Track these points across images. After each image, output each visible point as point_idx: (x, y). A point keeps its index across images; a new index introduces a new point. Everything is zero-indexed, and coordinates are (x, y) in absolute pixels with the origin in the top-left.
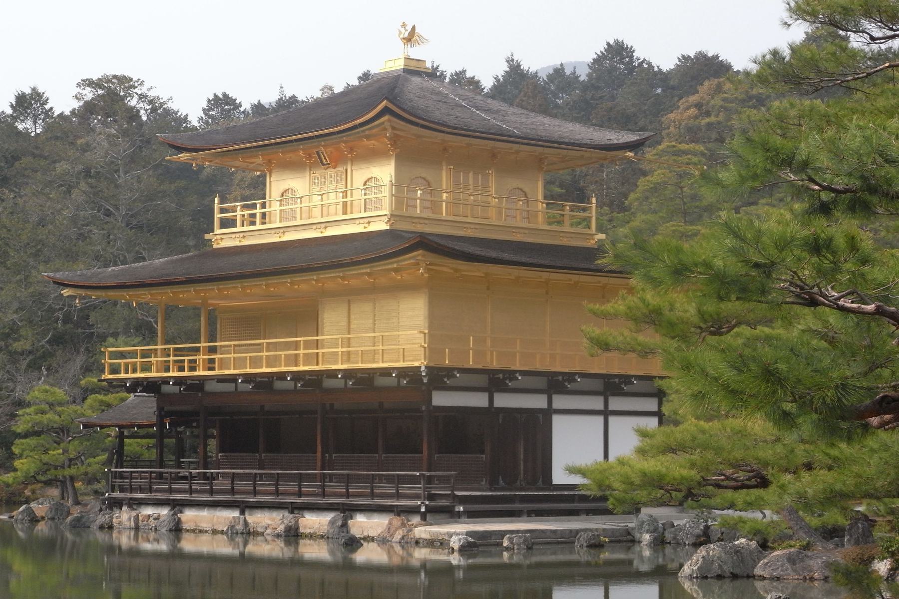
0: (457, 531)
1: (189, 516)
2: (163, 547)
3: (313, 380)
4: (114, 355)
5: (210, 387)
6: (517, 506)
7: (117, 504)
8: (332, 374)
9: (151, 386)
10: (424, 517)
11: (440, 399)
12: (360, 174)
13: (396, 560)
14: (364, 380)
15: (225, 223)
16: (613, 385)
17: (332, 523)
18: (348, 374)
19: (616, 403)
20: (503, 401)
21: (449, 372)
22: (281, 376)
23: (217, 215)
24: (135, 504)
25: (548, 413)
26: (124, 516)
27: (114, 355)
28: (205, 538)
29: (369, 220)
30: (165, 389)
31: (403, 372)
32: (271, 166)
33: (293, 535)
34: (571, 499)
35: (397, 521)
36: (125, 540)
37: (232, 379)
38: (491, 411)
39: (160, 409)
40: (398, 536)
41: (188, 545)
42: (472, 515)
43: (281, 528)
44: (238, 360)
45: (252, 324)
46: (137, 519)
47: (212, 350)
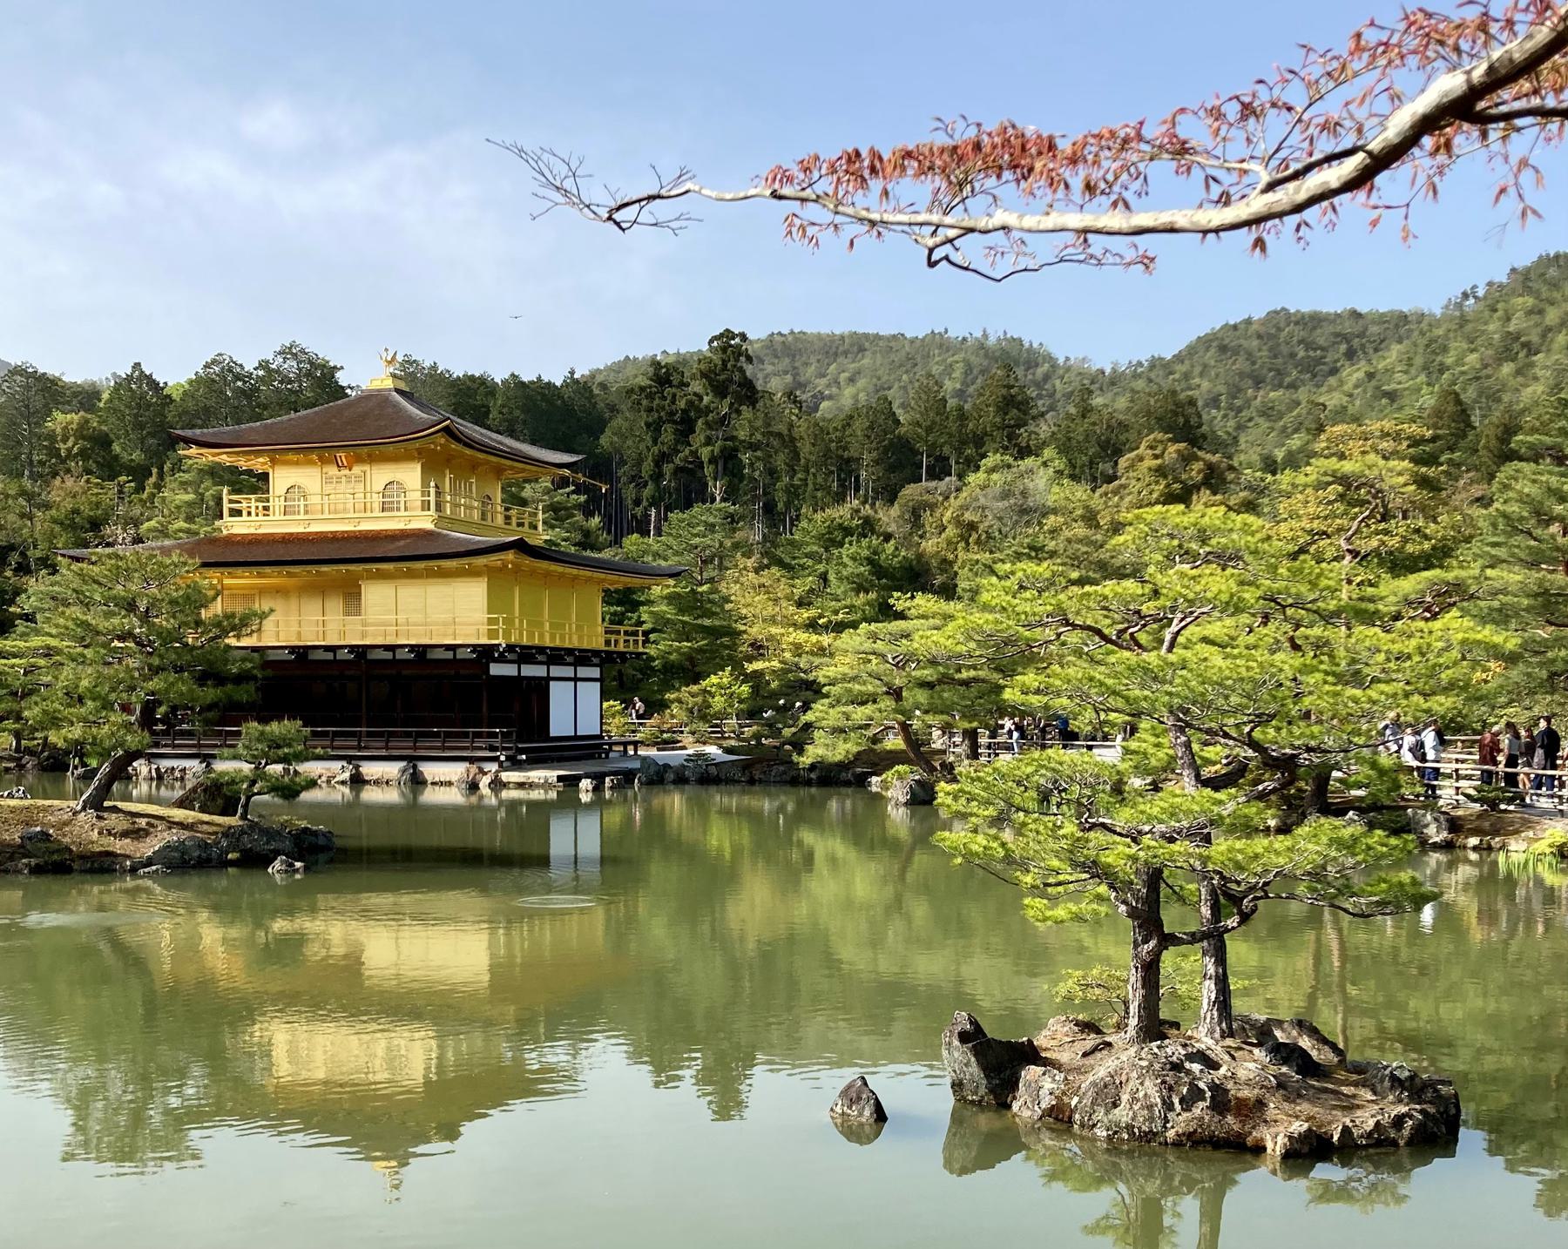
3: (360, 651)
11: (496, 669)
12: (381, 475)
14: (420, 650)
17: (404, 771)
18: (412, 648)
19: (583, 672)
20: (529, 671)
23: (226, 506)
24: (151, 757)
25: (549, 679)
29: (410, 519)
32: (274, 462)
33: (357, 781)
35: (474, 769)
38: (519, 678)
40: (485, 781)
43: (346, 776)
46: (158, 769)
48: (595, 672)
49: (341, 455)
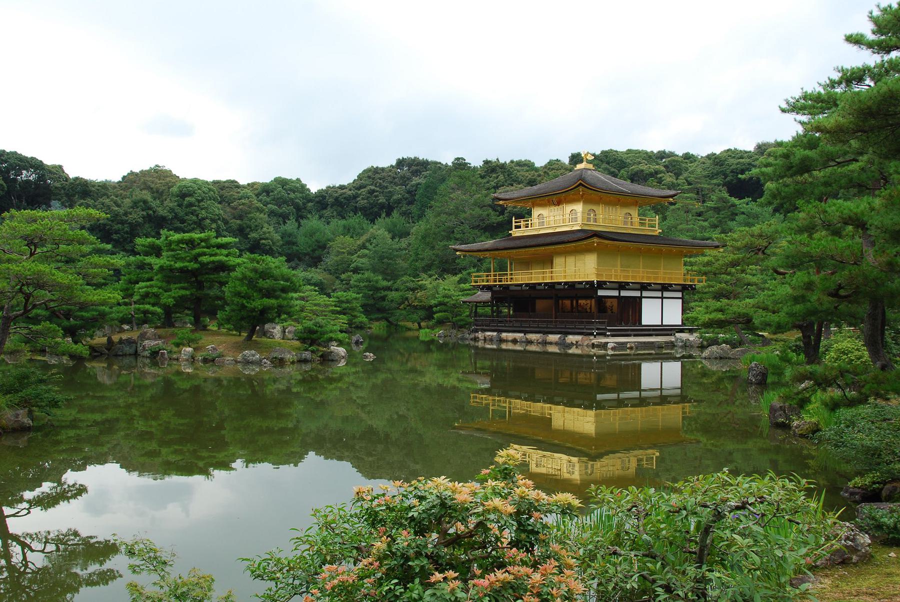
0: (612, 341)
1: (504, 335)
2: (495, 347)
3: (552, 285)
4: (475, 277)
5: (512, 288)
6: (629, 333)
7: (476, 331)
8: (560, 283)
9: (489, 288)
10: (595, 336)
11: (601, 293)
12: (568, 208)
13: (585, 352)
14: (572, 285)
15: (518, 227)
16: (665, 288)
18: (566, 283)
19: (666, 294)
20: (624, 293)
21: (605, 283)
22: (540, 284)
23: (514, 224)
24: (484, 331)
25: (641, 298)
26: (480, 335)
27: (475, 277)
28: (510, 344)
30: (494, 289)
31: (587, 282)
32: (534, 205)
34: (649, 330)
35: (585, 338)
36: (480, 344)
37: (521, 285)
38: (619, 298)
39: (492, 295)
41: (504, 346)
42: (613, 336)
43: (540, 340)
44: (521, 277)
45: (527, 264)
47: (511, 274)
48: (679, 295)
49: (555, 198)
